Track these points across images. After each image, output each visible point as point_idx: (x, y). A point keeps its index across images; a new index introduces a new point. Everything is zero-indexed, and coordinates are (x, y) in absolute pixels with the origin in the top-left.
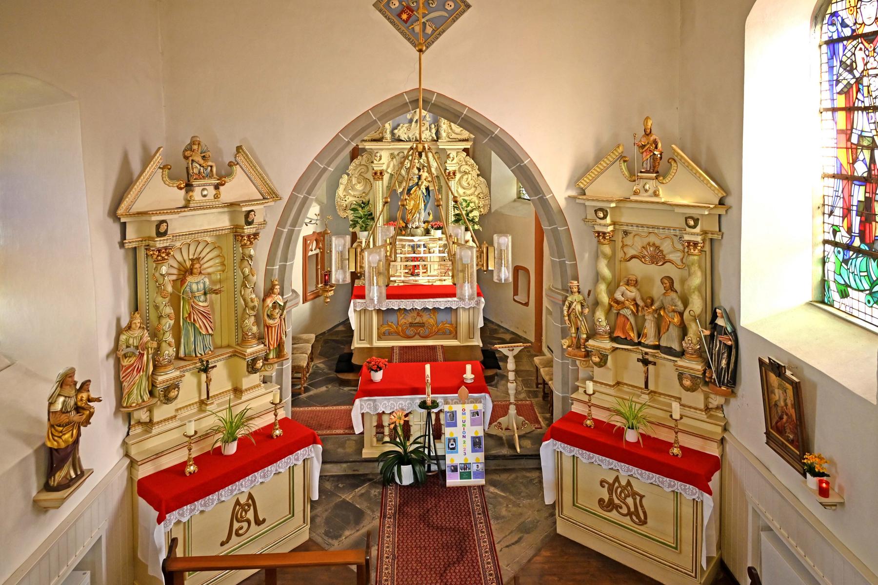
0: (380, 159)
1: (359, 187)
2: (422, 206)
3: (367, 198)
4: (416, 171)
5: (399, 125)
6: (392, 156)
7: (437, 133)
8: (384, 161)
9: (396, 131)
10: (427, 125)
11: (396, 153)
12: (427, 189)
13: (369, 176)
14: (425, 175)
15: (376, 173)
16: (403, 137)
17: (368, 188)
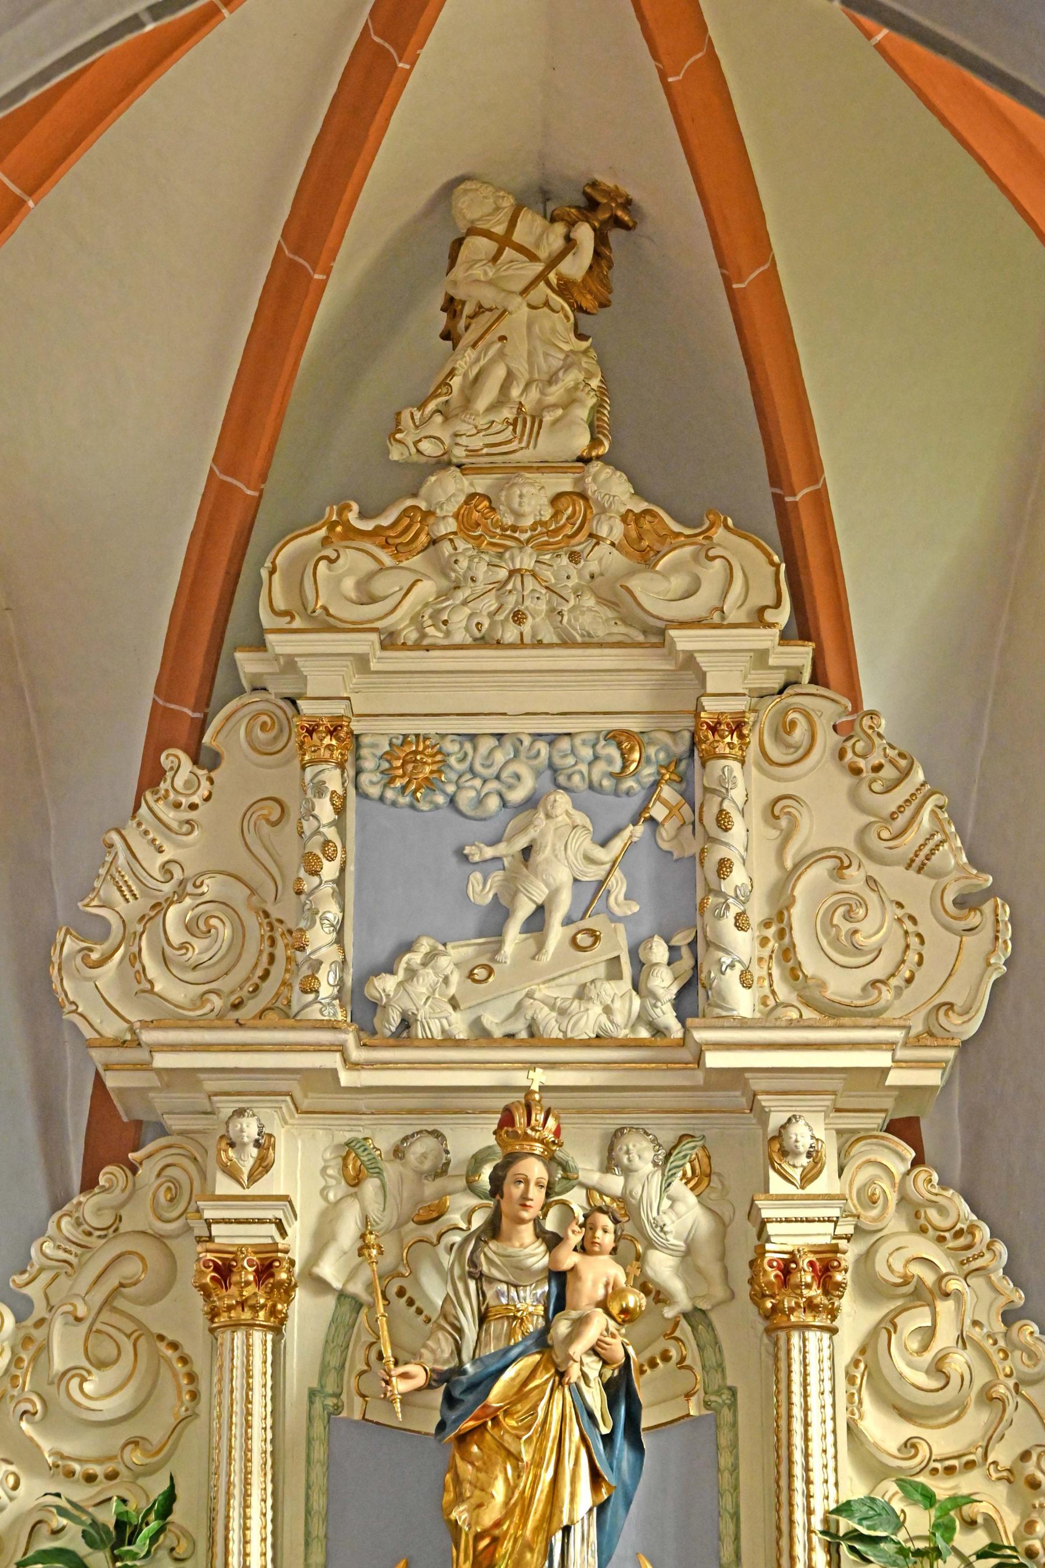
0: (263, 1166)
1: (99, 1394)
2: (580, 1501)
3: (158, 1487)
4: (537, 1256)
5: (408, 947)
6: (355, 1167)
7: (693, 995)
8: (295, 1186)
9: (387, 984)
10: (617, 942)
11: (384, 1139)
12: (620, 1389)
13: (183, 1312)
14: (598, 1274)
15: (224, 1272)
16: (434, 1021)
17: (170, 1403)
